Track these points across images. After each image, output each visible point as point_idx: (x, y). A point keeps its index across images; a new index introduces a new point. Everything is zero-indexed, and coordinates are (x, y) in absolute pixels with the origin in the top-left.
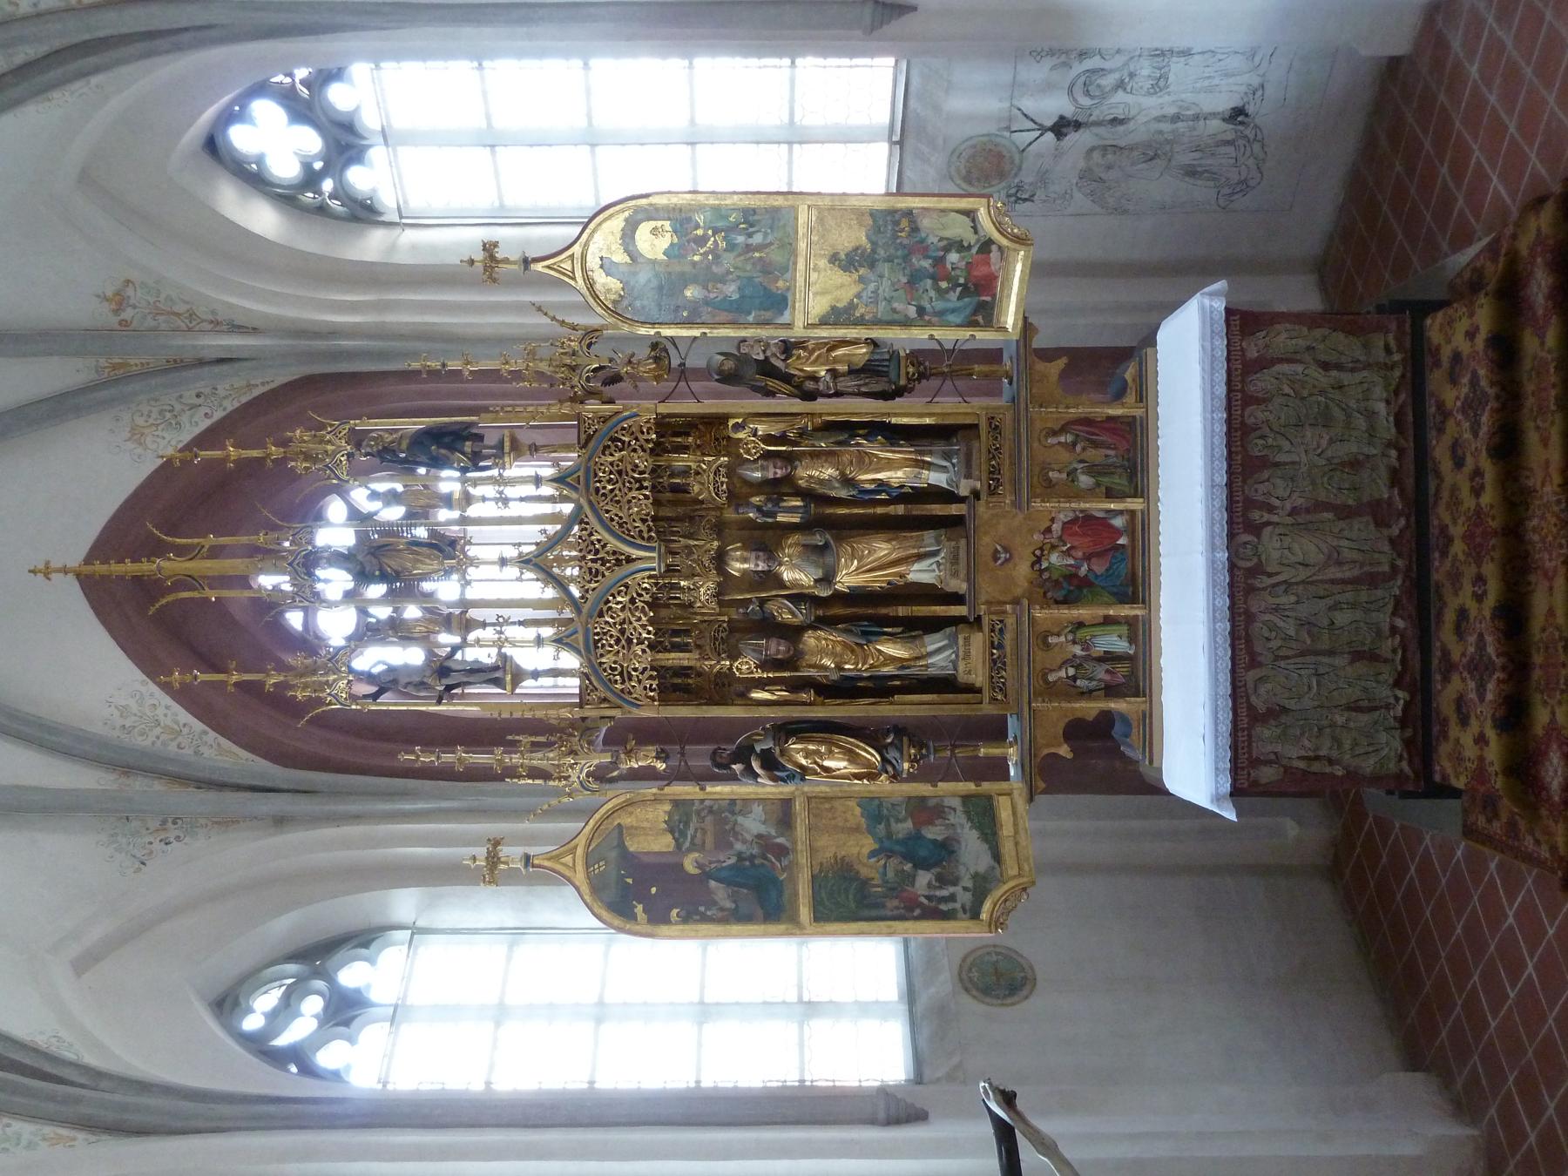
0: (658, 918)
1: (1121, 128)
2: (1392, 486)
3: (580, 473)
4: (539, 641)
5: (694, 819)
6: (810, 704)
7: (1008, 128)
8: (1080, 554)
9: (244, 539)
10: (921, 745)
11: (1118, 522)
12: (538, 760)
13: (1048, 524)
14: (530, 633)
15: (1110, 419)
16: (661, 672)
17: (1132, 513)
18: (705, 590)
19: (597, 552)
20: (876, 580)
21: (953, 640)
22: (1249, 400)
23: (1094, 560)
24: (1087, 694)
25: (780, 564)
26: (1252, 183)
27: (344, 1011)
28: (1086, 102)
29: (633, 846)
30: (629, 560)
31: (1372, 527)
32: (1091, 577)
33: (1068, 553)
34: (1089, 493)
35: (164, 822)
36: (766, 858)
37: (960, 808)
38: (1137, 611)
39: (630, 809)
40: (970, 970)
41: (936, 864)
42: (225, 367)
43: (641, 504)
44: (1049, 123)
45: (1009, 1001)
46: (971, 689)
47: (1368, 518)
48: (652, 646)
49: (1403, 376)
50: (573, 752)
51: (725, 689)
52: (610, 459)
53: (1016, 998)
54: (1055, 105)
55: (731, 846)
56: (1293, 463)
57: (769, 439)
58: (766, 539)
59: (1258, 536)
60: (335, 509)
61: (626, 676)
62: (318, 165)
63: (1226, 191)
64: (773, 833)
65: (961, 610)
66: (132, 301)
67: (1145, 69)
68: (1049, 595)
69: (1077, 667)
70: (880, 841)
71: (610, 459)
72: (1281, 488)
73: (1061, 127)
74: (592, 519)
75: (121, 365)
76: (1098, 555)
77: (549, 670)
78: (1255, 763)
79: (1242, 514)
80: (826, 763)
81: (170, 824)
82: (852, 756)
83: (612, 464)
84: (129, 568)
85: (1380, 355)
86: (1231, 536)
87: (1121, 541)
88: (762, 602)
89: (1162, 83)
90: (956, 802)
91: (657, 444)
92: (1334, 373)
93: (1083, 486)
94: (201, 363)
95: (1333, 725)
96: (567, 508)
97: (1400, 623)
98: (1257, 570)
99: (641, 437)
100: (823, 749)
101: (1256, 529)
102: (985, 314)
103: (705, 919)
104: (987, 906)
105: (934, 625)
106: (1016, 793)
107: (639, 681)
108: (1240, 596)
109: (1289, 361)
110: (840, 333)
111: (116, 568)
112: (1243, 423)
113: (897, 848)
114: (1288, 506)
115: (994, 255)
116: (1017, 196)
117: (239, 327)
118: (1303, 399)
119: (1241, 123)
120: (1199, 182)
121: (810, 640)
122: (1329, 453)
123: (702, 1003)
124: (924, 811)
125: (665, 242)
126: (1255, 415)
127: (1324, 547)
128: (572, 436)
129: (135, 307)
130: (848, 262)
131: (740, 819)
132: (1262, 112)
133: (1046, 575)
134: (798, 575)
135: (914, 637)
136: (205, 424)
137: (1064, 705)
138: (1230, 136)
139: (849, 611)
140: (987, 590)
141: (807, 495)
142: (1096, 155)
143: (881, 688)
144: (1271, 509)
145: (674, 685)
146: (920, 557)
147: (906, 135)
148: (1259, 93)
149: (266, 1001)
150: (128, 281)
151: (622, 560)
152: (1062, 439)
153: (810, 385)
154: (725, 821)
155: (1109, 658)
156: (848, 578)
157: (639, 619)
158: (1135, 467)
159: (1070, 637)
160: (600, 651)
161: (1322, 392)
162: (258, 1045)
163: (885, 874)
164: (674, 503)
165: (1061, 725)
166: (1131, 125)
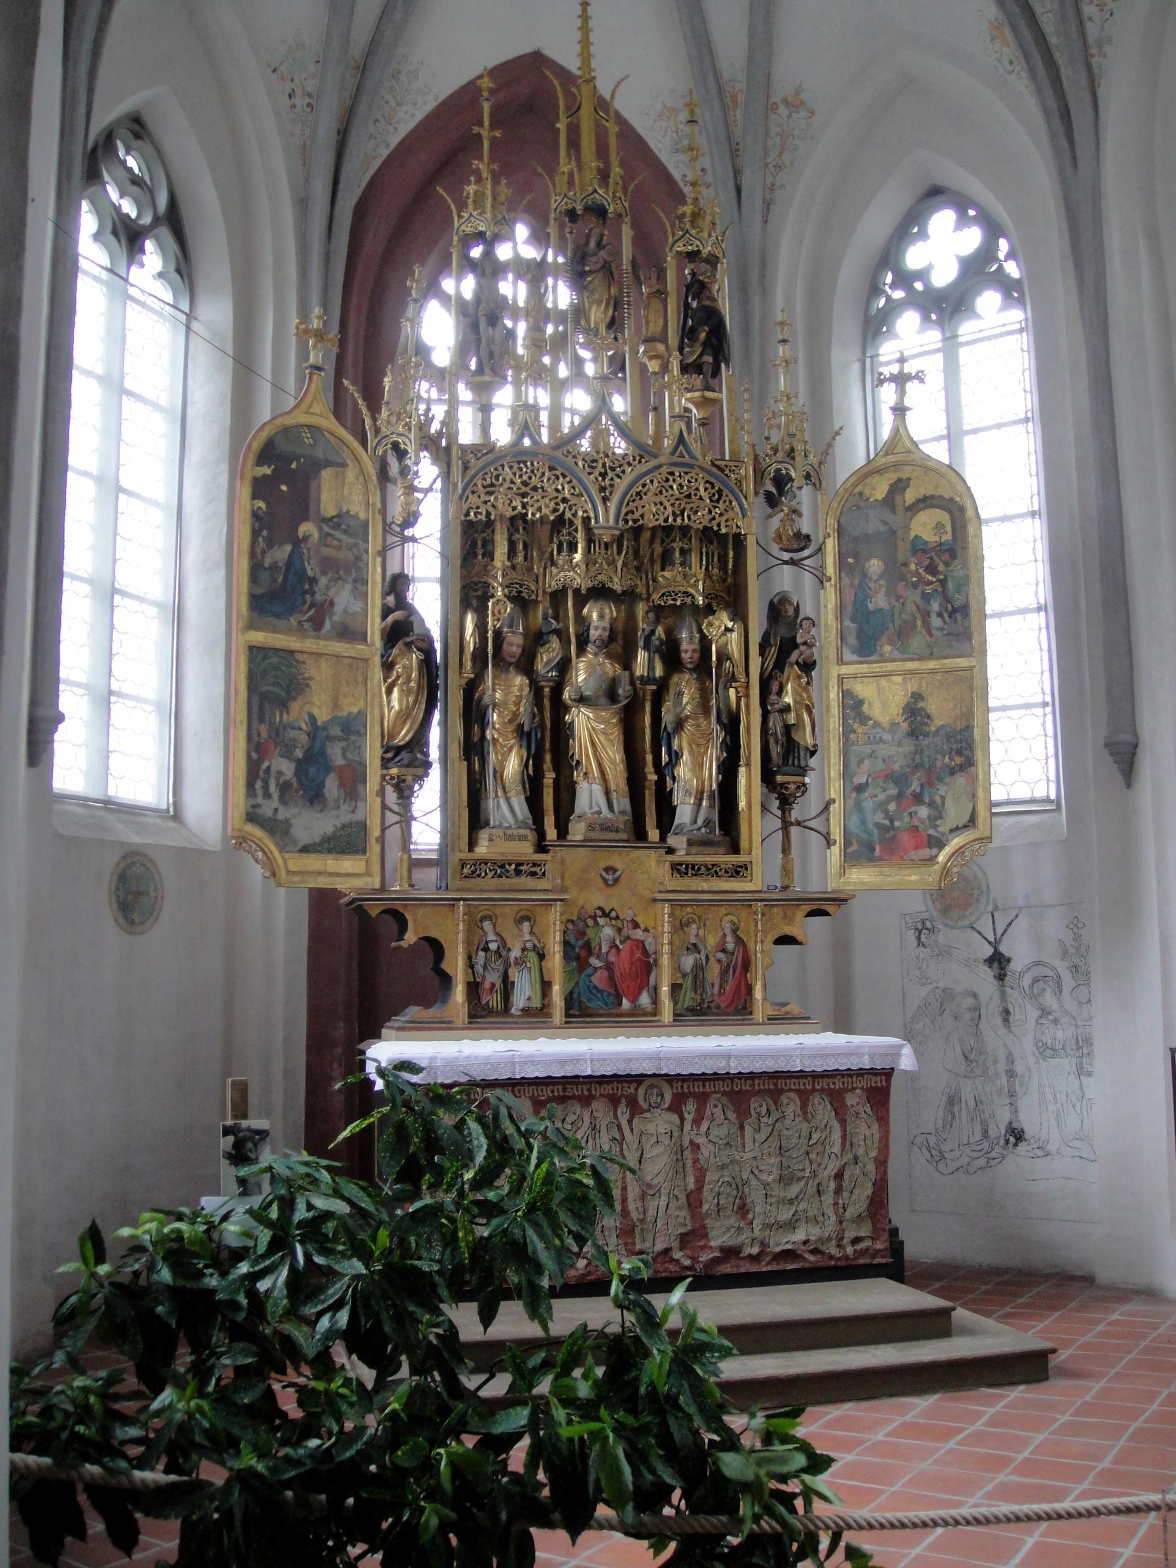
0: (260, 488)
1: (999, 1021)
2: (722, 1249)
3: (687, 459)
5: (350, 541)
6: (461, 673)
7: (996, 908)
8: (612, 958)
11: (645, 999)
13: (642, 926)
15: (750, 990)
17: (655, 1012)
19: (613, 469)
21: (523, 825)
22: (805, 1096)
23: (606, 973)
24: (471, 966)
25: (595, 655)
26: (941, 1165)
28: (1026, 981)
29: (326, 474)
30: (605, 500)
31: (683, 1230)
32: (589, 971)
34: (677, 968)
35: (310, 95)
36: (312, 605)
37: (355, 817)
39: (361, 478)
40: (142, 865)
41: (299, 781)
44: (1003, 949)
45: (114, 901)
46: (472, 844)
47: (689, 1228)
49: (831, 1257)
52: (702, 489)
53: (115, 906)
55: (324, 573)
56: (744, 1146)
58: (620, 645)
59: (669, 1109)
61: (490, 488)
62: (919, 286)
63: (932, 1140)
64: (336, 618)
65: (551, 833)
66: (794, 115)
68: (571, 926)
69: (498, 952)
71: (702, 489)
72: (720, 1132)
73: (998, 961)
75: (735, 103)
76: (611, 979)
80: (396, 690)
81: (307, 100)
83: (697, 489)
85: (850, 1234)
86: (670, 1079)
87: (625, 1002)
89: (1048, 1053)
90: (359, 816)
92: (832, 1185)
93: (683, 959)
94: (737, 172)
98: (635, 1108)
99: (724, 518)
100: (413, 684)
106: (369, 879)
107: (486, 502)
108: (607, 1089)
109: (844, 1137)
112: (782, 1091)
113: (317, 745)
114: (701, 1140)
116: (922, 930)
117: (768, 209)
118: (807, 1153)
119: (1007, 1142)
120: (941, 1113)
121: (519, 681)
122: (754, 1182)
126: (790, 1103)
127: (660, 1178)
129: (790, 116)
131: (349, 587)
132: (1019, 1160)
133: (590, 922)
134: (581, 674)
135: (524, 787)
136: (676, 174)
137: (460, 936)
138: (992, 1133)
139: (548, 723)
140: (576, 859)
142: (969, 1001)
144: (697, 1122)
146: (607, 793)
148: (1040, 1153)
150: (812, 113)
151: (605, 494)
152: (729, 939)
153: (775, 687)
154: (348, 571)
155: (507, 987)
157: (547, 506)
158: (705, 1014)
159: (529, 945)
160: (516, 466)
161: (814, 1174)
163: (293, 728)
165: (433, 934)
166: (1002, 1030)
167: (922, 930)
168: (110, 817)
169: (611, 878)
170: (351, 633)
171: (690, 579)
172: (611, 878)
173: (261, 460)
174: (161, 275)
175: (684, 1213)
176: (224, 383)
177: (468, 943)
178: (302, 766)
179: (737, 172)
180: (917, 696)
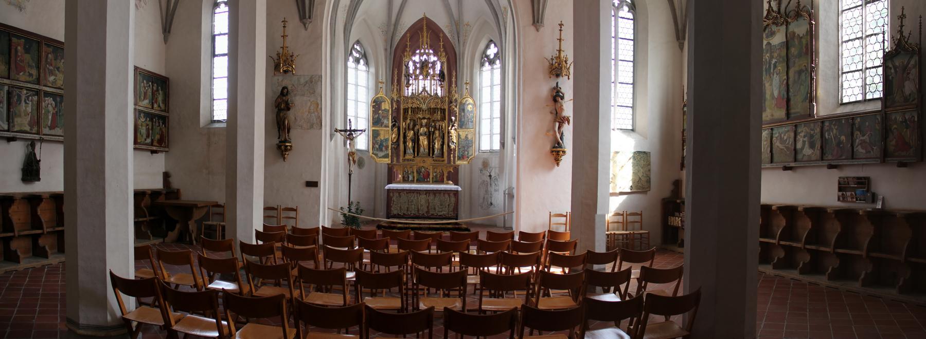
0: (373, 107)
18: (421, 116)
20: (421, 142)
43: (433, 106)
51: (405, 119)
58: (428, 126)
60: (435, 59)
77: (409, 91)
102: (459, 159)
124: (387, 147)
130: (466, 137)
143: (405, 142)
145: (406, 110)
147: (492, 152)
156: (421, 138)
167: (481, 170)
169: (424, 162)
170: (387, 126)
171: (438, 116)
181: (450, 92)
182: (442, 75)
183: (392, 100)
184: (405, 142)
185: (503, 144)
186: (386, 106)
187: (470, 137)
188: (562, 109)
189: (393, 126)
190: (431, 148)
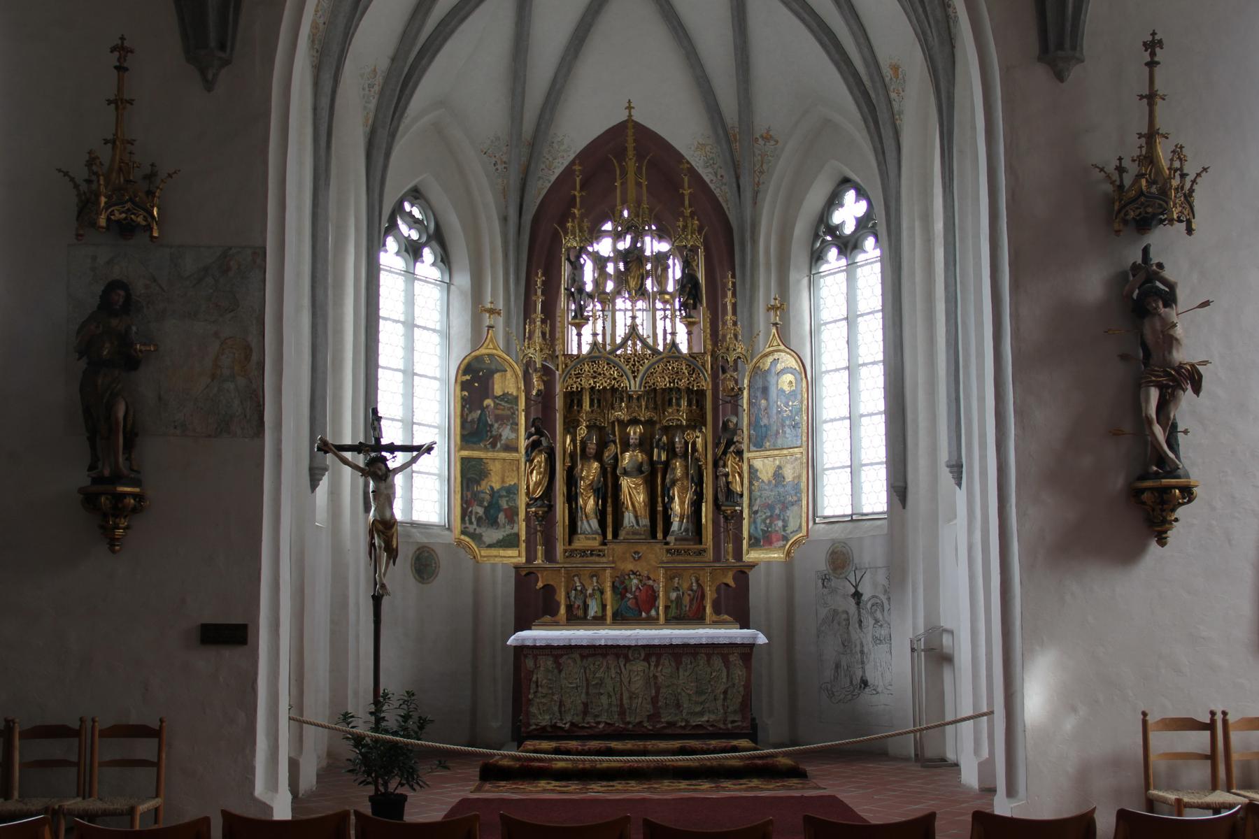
0: (464, 386)
2: (668, 723)
4: (595, 335)
9: (645, 198)
10: (543, 518)
11: (653, 613)
12: (538, 333)
14: (599, 330)
15: (704, 608)
16: (580, 393)
17: (658, 619)
18: (622, 414)
22: (709, 656)
27: (412, 251)
29: (497, 376)
30: (635, 377)
33: (638, 588)
34: (667, 597)
38: (609, 620)
42: (735, 189)
44: (859, 589)
46: (570, 543)
48: (592, 388)
50: (541, 350)
51: (571, 425)
54: (867, 590)
57: (694, 444)
58: (645, 444)
61: (578, 376)
65: (610, 536)
67: (884, 632)
70: (498, 491)
73: (857, 595)
74: (655, 359)
76: (637, 603)
77: (580, 341)
78: (535, 657)
79: (651, 652)
82: (537, 484)
84: (631, 145)
85: (730, 719)
88: (614, 442)
90: (515, 530)
91: (692, 391)
94: (738, 178)
95: (553, 694)
96: (661, 348)
97: (601, 726)
98: (627, 660)
101: (647, 659)
102: (755, 543)
103: (463, 407)
104: (467, 539)
105: (602, 524)
110: (746, 475)
111: (630, 140)
115: (782, 543)
121: (596, 465)
123: (413, 423)
124: (512, 514)
125: (787, 388)
126: (702, 660)
128: (695, 350)
136: (707, 179)
140: (619, 549)
141: (667, 465)
143: (571, 498)
144: (657, 666)
146: (636, 517)
147: (855, 519)
149: (416, 212)
153: (721, 463)
155: (586, 607)
156: (626, 483)
161: (713, 691)
162: (398, 209)
164: (663, 399)
168: (414, 530)
171: (680, 413)
172: (637, 557)
173: (466, 372)
174: (433, 264)
175: (649, 707)
176: (467, 317)
177: (567, 587)
178: (487, 510)
179: (738, 178)
180: (780, 467)
181: (715, 336)
182: (689, 287)
183: (528, 366)
184: (571, 498)
185: (899, 490)
186: (507, 384)
187: (789, 473)
188: (1170, 341)
189: (533, 447)
190: (658, 515)
